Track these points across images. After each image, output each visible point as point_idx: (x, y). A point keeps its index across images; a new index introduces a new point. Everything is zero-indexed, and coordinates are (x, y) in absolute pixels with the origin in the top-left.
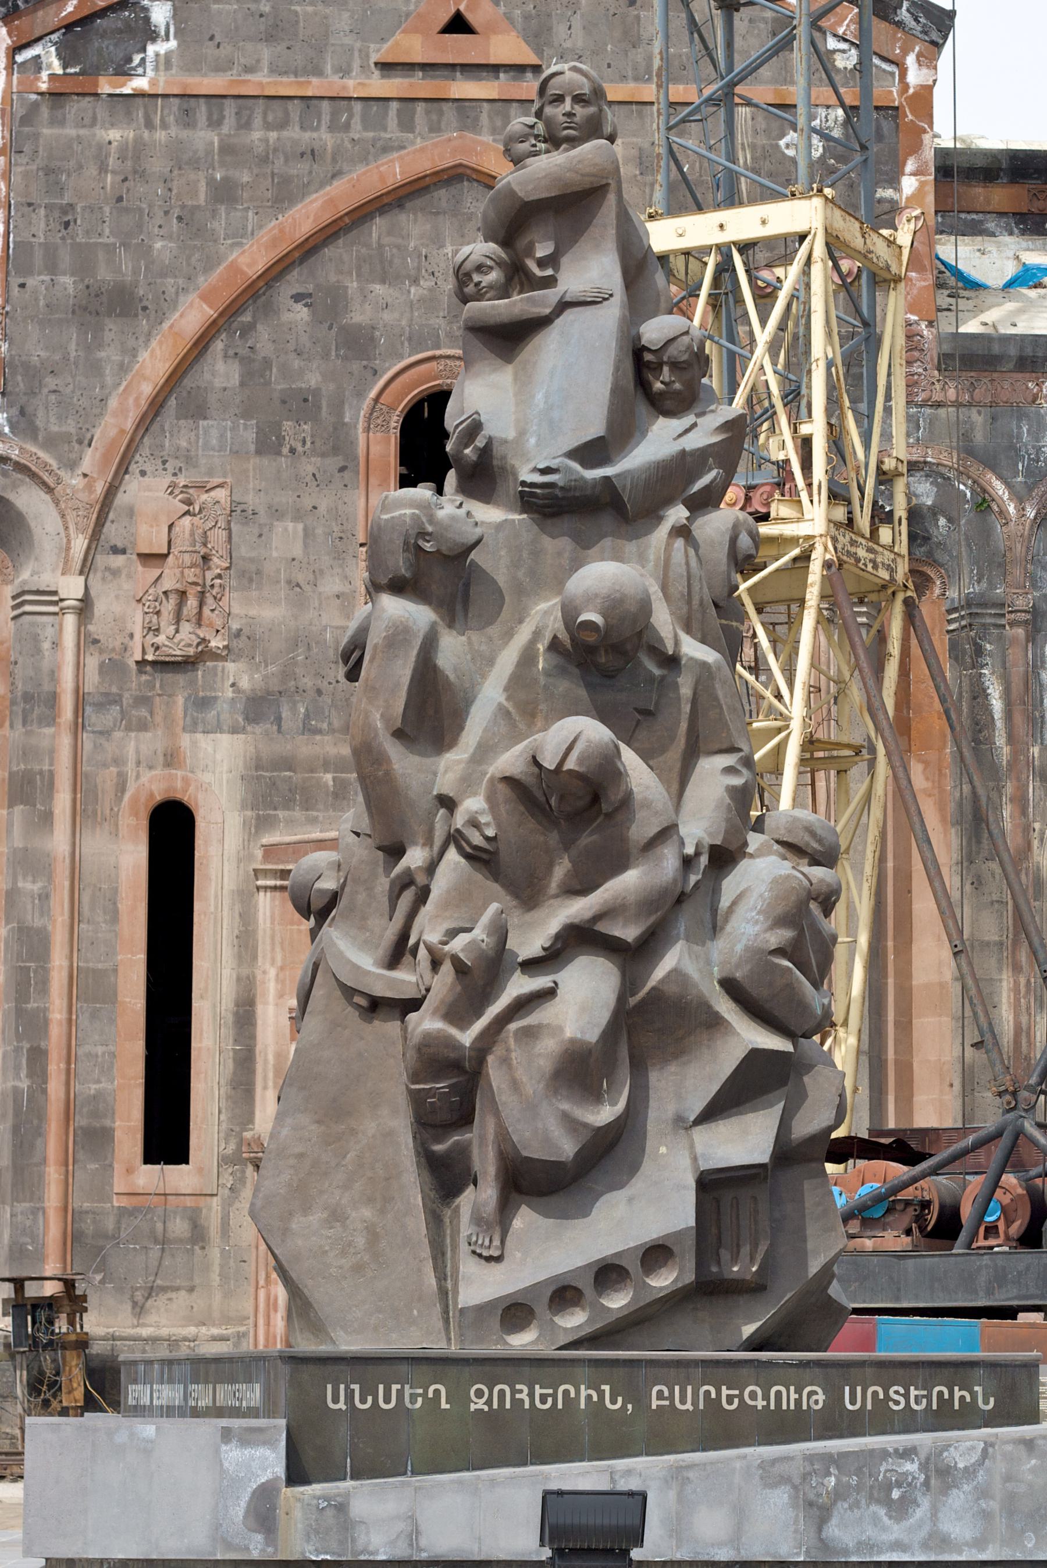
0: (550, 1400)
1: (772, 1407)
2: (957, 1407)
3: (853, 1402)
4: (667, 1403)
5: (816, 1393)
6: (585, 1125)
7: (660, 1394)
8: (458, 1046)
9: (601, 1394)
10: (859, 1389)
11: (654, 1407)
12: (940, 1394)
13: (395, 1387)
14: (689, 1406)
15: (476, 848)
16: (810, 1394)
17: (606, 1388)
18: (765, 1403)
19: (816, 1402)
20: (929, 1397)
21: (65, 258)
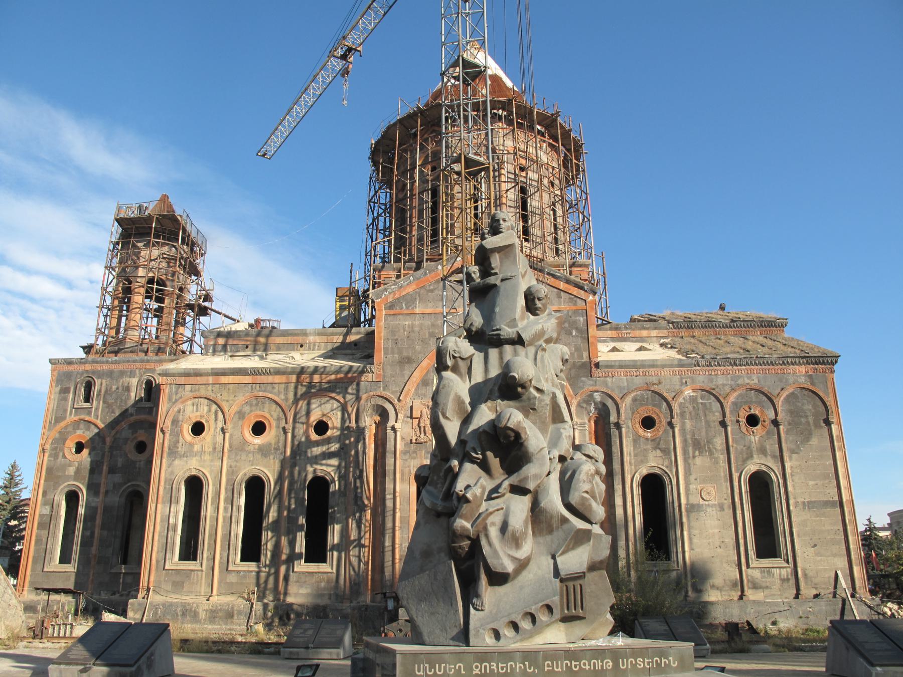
3: (623, 665)
6: (516, 559)
9: (525, 666)
13: (443, 665)
14: (560, 669)
17: (527, 663)
20: (652, 662)
21: (396, 351)
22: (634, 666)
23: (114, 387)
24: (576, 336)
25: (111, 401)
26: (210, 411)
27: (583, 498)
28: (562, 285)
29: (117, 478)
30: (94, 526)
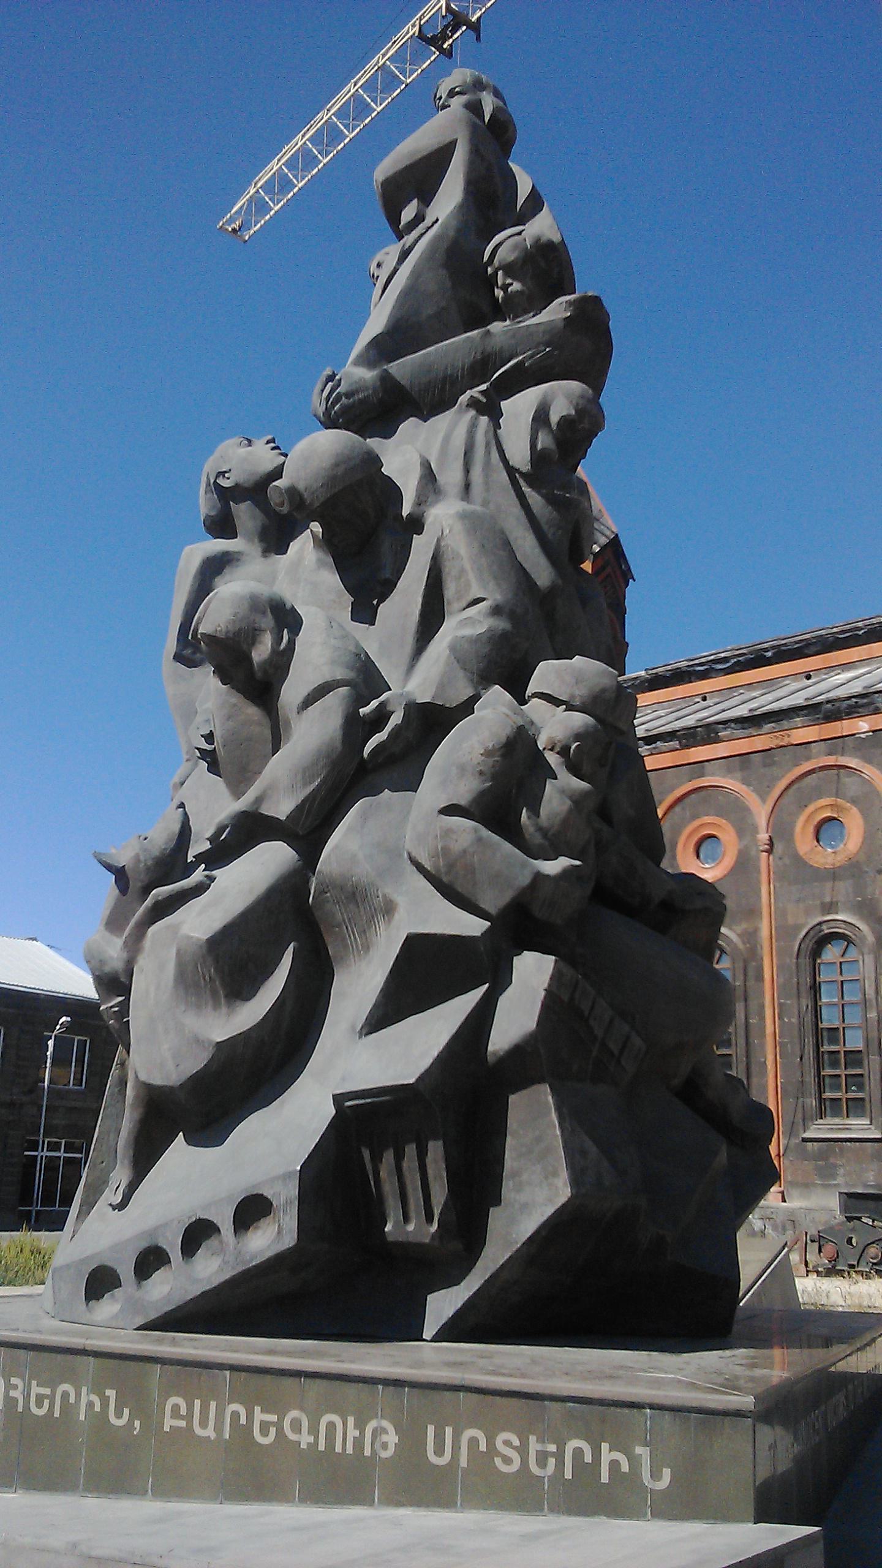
0: (46, 1402)
1: (322, 1447)
2: (605, 1478)
3: (439, 1451)
4: (183, 1424)
5: (384, 1431)
7: (176, 1412)
10: (449, 1431)
11: (167, 1429)
12: (578, 1453)
14: (210, 1432)
16: (375, 1433)
17: (111, 1393)
18: (311, 1439)
19: (385, 1446)
22: (483, 1460)
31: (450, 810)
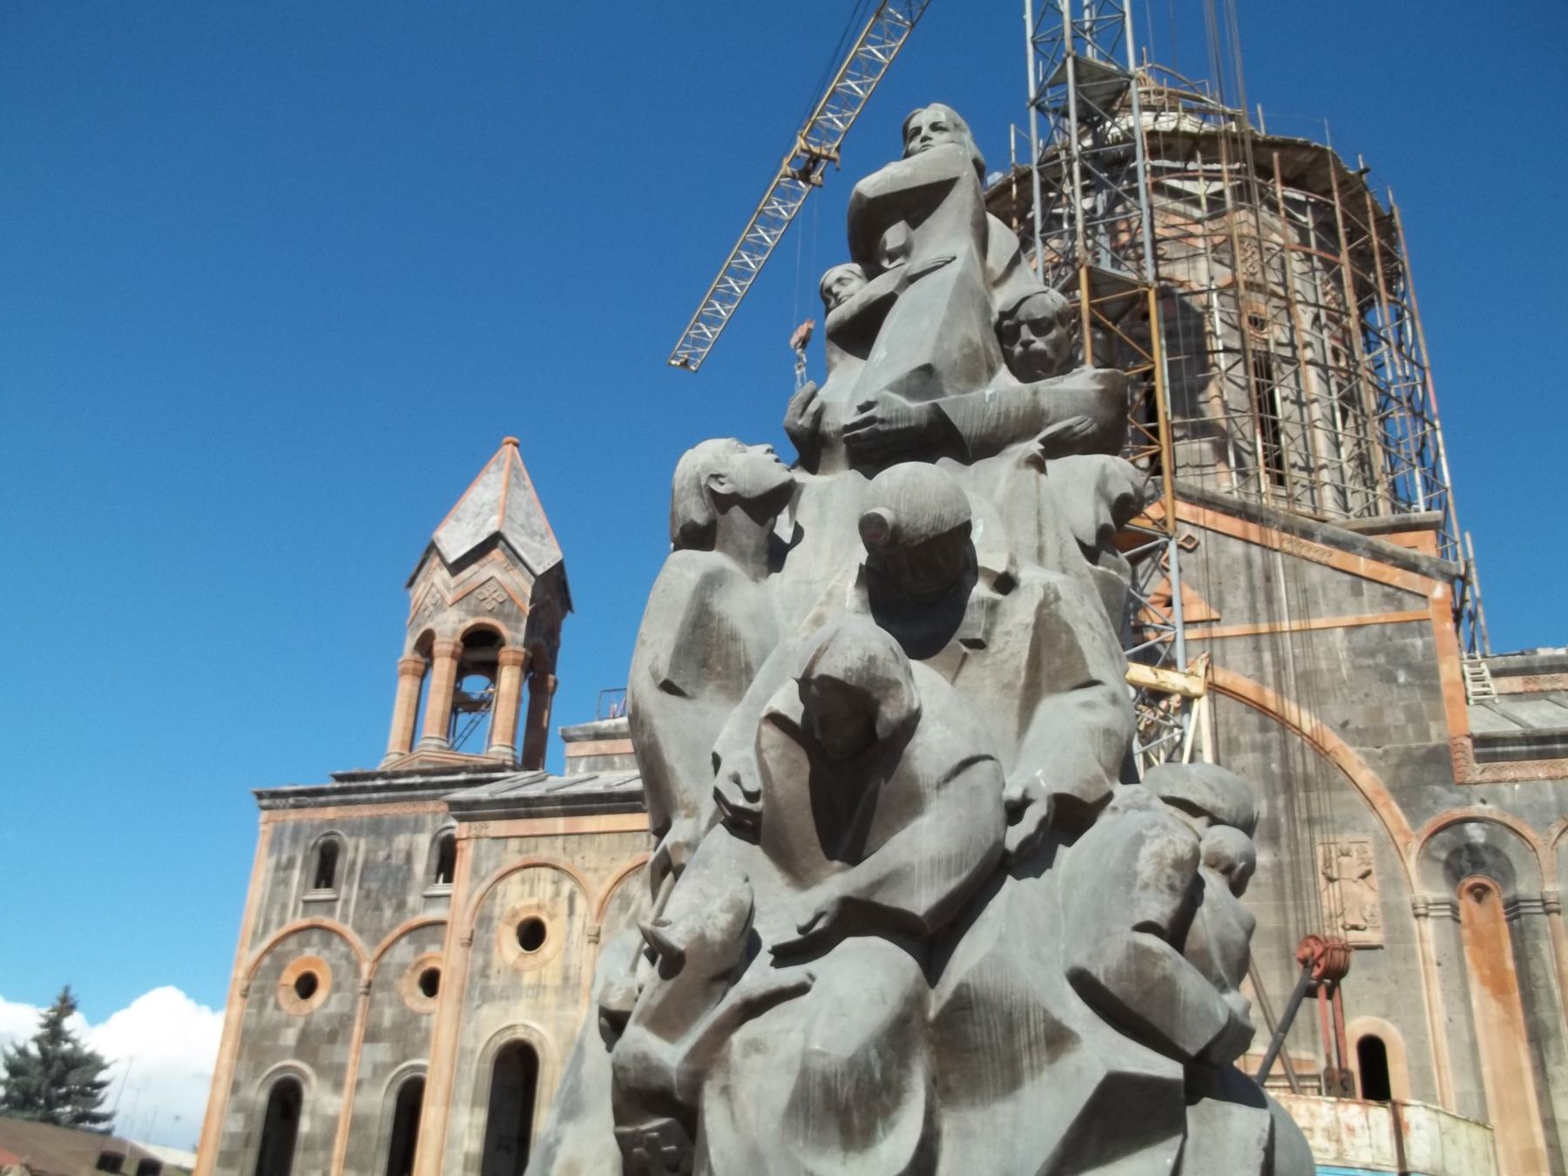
8: (659, 1070)
15: (735, 809)
23: (382, 855)
24: (1408, 685)
25: (374, 886)
26: (557, 894)
27: (1141, 953)
28: (1363, 565)
29: (382, 1052)
30: (329, 1161)
31: (1146, 927)
